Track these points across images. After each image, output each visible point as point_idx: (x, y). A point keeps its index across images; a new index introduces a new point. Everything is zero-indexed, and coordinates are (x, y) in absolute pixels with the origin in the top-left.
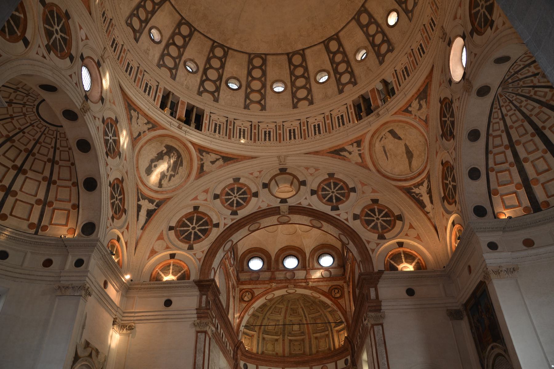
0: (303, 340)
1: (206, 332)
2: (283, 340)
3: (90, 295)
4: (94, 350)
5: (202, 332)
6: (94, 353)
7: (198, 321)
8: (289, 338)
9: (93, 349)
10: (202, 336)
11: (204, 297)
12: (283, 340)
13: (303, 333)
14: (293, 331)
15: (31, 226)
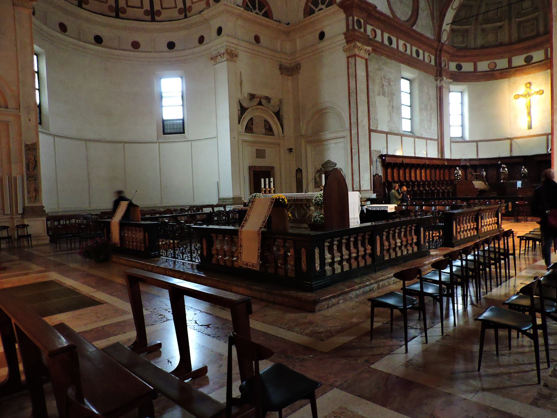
0: (536, 18)
1: (355, 56)
2: (510, 25)
3: (236, 56)
4: (263, 98)
5: (351, 56)
6: (263, 101)
7: (347, 46)
8: (518, 20)
9: (261, 98)
10: (352, 60)
11: (351, 18)
12: (510, 25)
13: (536, 9)
14: (523, 10)
15: (180, 11)
